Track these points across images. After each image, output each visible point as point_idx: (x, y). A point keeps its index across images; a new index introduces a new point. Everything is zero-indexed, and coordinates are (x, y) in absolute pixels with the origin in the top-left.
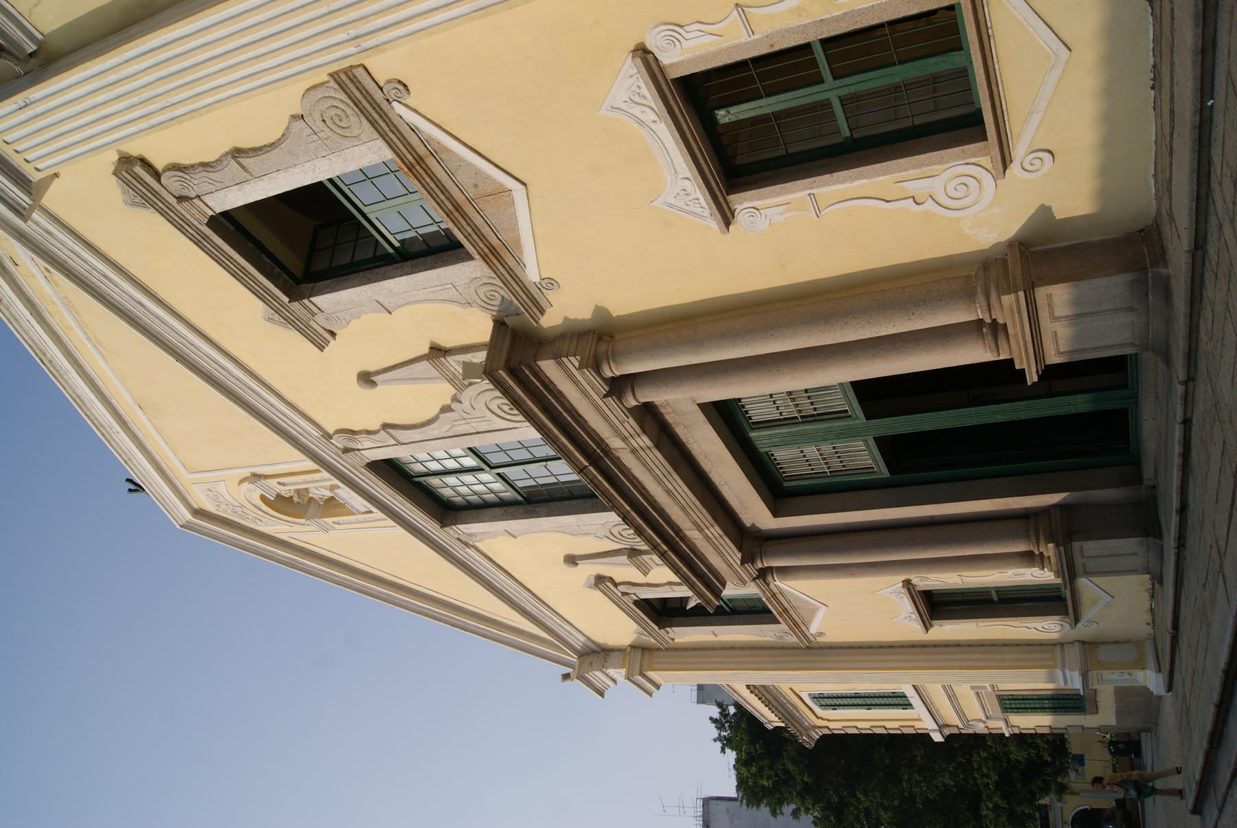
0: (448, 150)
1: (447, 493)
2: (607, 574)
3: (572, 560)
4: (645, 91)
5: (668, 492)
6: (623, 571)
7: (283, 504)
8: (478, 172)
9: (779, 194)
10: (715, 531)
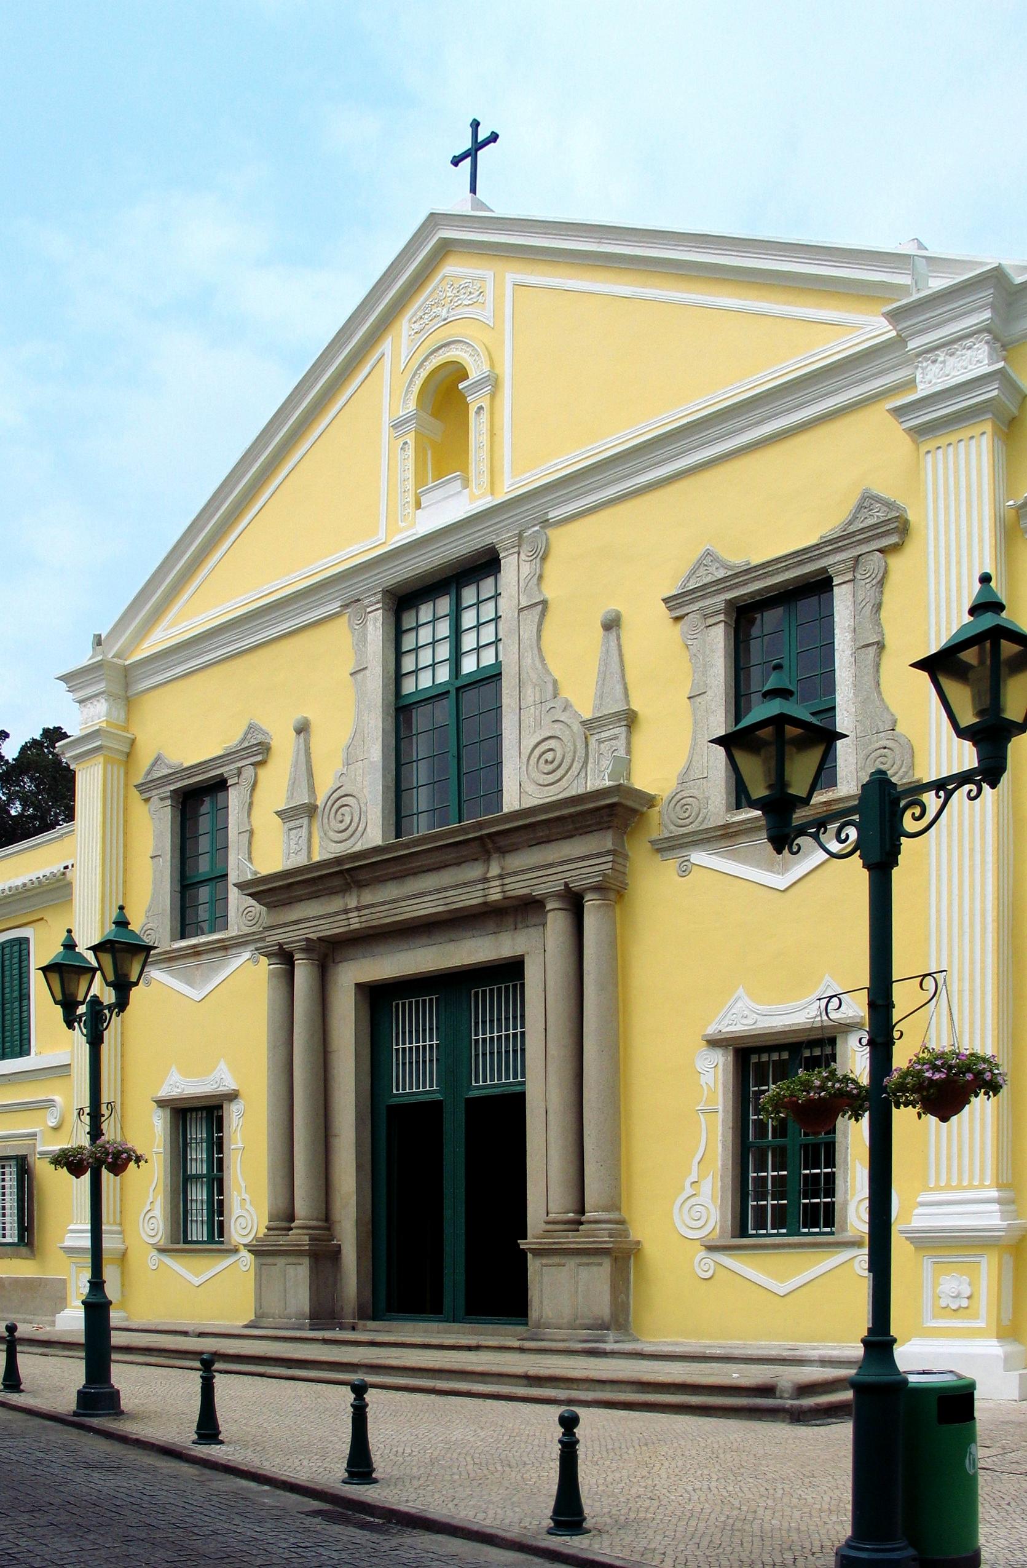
1: (425, 612)
6: (274, 787)
9: (724, 1087)
10: (355, 922)
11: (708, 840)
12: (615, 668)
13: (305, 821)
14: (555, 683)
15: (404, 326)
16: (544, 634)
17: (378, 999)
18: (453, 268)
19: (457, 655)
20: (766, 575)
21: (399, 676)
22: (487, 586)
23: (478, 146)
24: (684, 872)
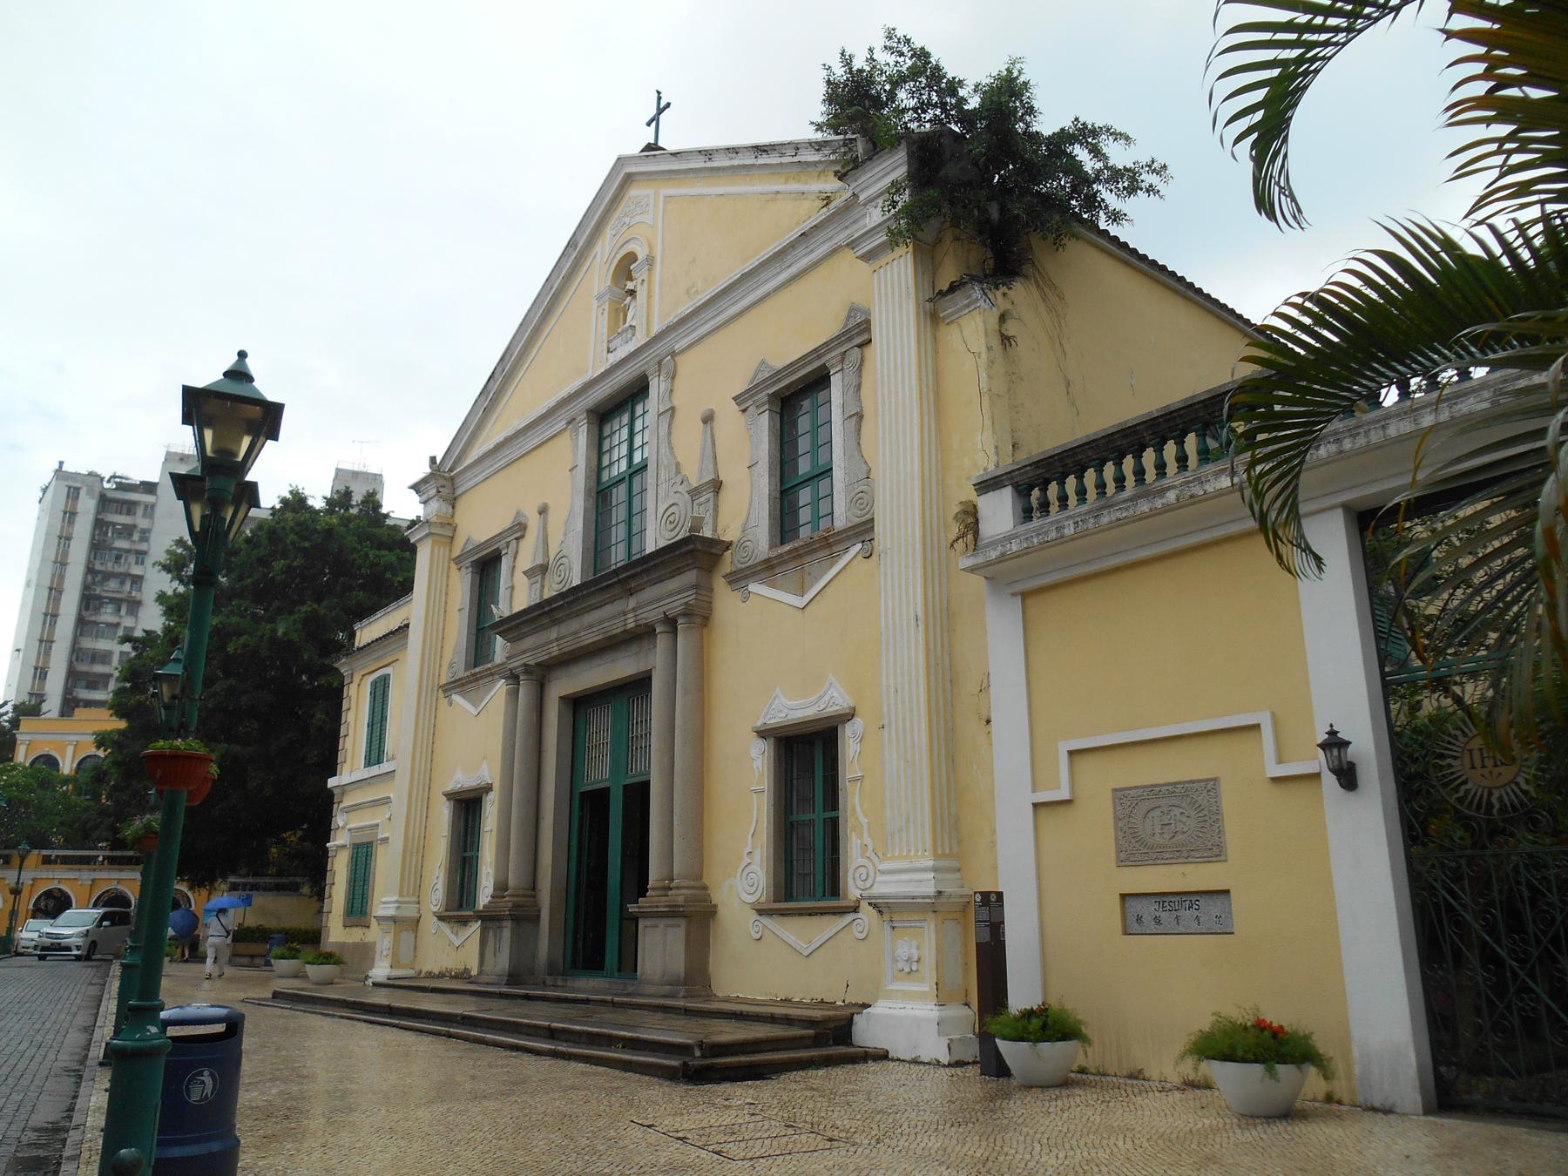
0: (832, 565)
2: (528, 534)
3: (543, 511)
4: (835, 708)
5: (591, 626)
6: (527, 555)
7: (625, 268)
8: (817, 579)
10: (555, 650)
11: (754, 574)
12: (712, 452)
13: (539, 578)
14: (678, 464)
15: (608, 232)
16: (674, 431)
17: (578, 704)
18: (634, 192)
20: (798, 369)
21: (600, 469)
23: (660, 111)
24: (745, 599)
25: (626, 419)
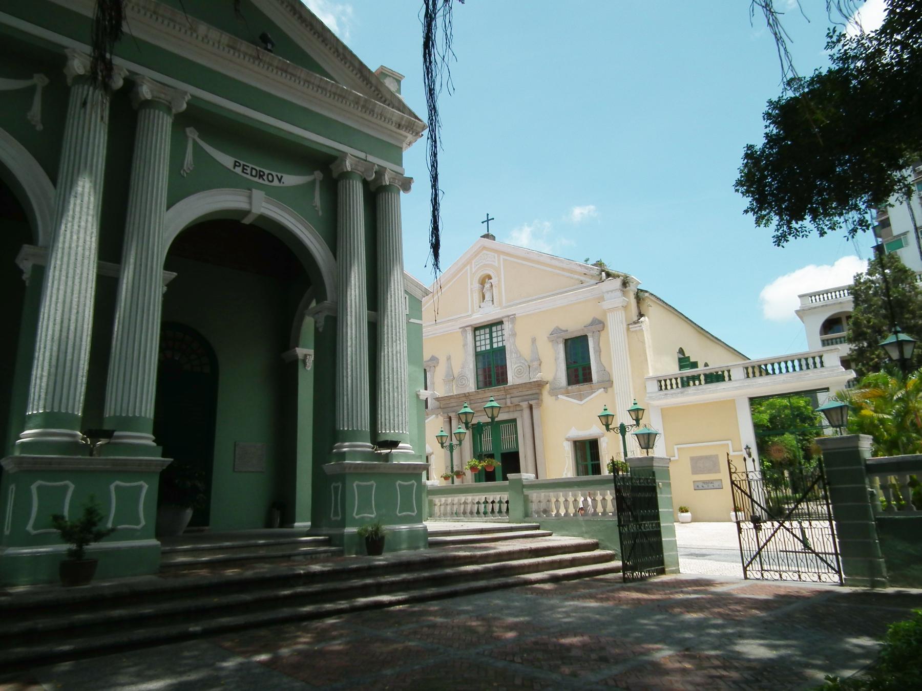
1: (482, 332)
3: (449, 359)
19: (491, 343)
22: (499, 327)
23: (488, 220)
25: (487, 330)
